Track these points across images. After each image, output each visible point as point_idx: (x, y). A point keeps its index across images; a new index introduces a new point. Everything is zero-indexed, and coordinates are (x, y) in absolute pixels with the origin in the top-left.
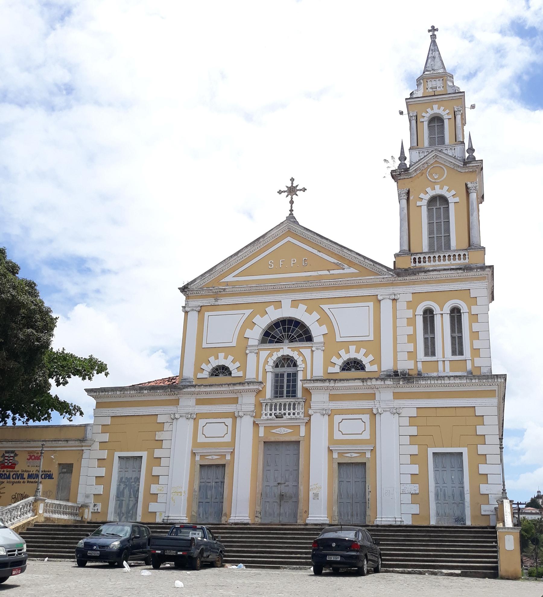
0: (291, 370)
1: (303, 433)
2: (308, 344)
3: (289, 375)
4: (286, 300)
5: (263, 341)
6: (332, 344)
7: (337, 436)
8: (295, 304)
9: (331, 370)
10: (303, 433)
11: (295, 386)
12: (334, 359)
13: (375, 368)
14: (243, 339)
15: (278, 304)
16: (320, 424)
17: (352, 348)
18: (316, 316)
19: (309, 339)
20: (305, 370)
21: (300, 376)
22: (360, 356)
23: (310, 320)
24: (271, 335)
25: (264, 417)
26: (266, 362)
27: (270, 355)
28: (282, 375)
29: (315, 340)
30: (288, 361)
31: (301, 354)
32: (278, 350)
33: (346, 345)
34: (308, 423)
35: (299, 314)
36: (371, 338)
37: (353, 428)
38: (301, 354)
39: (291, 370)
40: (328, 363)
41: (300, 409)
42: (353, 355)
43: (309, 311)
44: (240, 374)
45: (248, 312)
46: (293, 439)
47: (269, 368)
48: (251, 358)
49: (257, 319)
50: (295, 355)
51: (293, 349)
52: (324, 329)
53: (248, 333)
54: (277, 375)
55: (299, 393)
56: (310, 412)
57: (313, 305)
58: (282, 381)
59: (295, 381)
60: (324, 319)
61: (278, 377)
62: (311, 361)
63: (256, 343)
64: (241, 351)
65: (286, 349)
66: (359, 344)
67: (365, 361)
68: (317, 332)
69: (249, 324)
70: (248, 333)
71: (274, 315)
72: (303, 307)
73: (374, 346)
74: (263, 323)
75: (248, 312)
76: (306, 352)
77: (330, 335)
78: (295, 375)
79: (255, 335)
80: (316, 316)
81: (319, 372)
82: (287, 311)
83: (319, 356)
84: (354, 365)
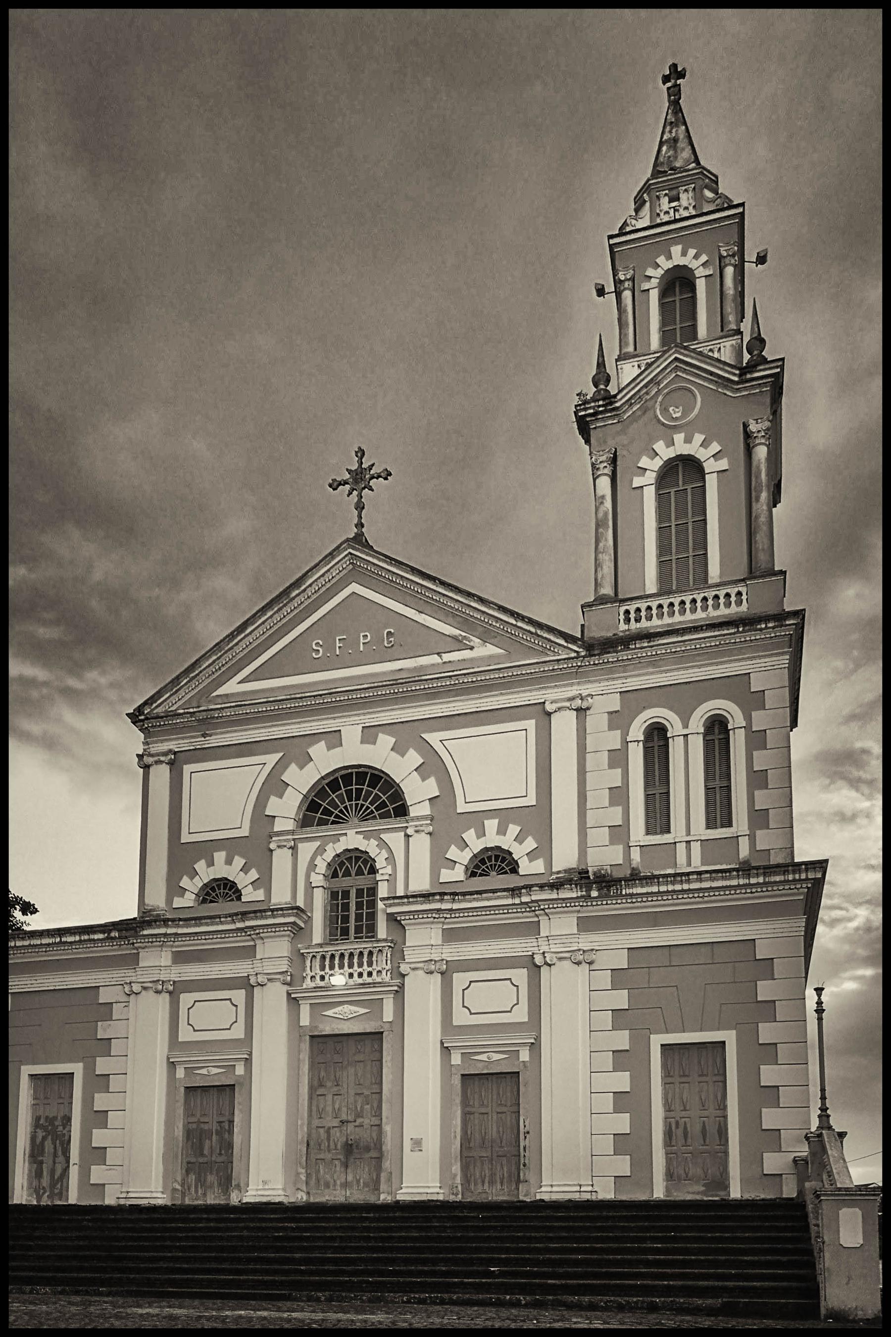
0: (363, 882)
1: (388, 1014)
2: (398, 823)
3: (360, 893)
4: (351, 728)
5: (305, 822)
6: (448, 821)
7: (460, 1017)
8: (369, 734)
9: (446, 875)
10: (388, 1014)
11: (372, 916)
12: (453, 853)
13: (538, 867)
14: (262, 819)
15: (334, 738)
16: (423, 992)
17: (491, 825)
18: (414, 758)
19: (402, 811)
20: (392, 880)
21: (383, 891)
22: (507, 842)
23: (402, 768)
24: (320, 808)
25: (308, 983)
26: (312, 866)
27: (321, 851)
28: (346, 894)
29: (413, 812)
30: (355, 863)
31: (383, 844)
32: (336, 839)
33: (476, 819)
34: (399, 993)
35: (380, 755)
36: (531, 800)
37: (494, 999)
38: (383, 844)
39: (363, 882)
40: (439, 860)
41: (382, 963)
42: (492, 839)
43: (399, 749)
44: (260, 895)
45: (272, 759)
46: (370, 1027)
47: (317, 879)
48: (281, 860)
49: (292, 774)
50: (371, 847)
51: (367, 835)
52: (431, 787)
53: (274, 806)
54: (334, 895)
55: (382, 931)
56: (404, 968)
57: (408, 736)
58: (346, 907)
59: (372, 904)
60: (433, 766)
61: (337, 900)
62: (407, 860)
63: (290, 825)
64: (257, 845)
65: (352, 838)
66: (505, 816)
67: (519, 852)
68: (418, 792)
69: (274, 785)
70: (274, 806)
71: (325, 761)
72: (386, 741)
73: (537, 819)
74: (302, 780)
75: (272, 759)
76: (395, 840)
77: (444, 800)
78: (373, 891)
79: (286, 809)
80: (414, 758)
81: (421, 882)
82: (353, 752)
83: (421, 845)
84: (495, 861)
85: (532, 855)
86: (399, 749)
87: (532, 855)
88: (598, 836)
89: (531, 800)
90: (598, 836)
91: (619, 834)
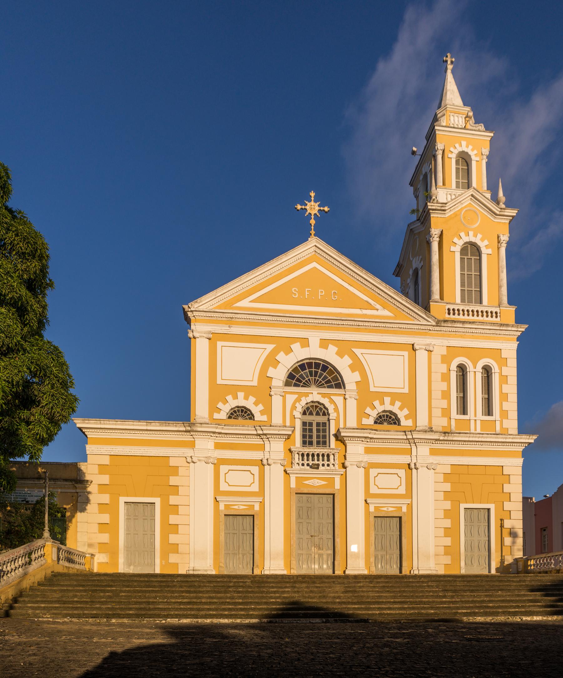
2: (341, 391)
4: (314, 337)
8: (324, 343)
20: (337, 420)
26: (294, 408)
27: (298, 400)
30: (316, 409)
31: (332, 401)
32: (307, 395)
33: (380, 396)
36: (406, 390)
38: (332, 401)
39: (321, 419)
40: (361, 414)
43: (340, 354)
48: (277, 401)
50: (325, 401)
51: (324, 395)
53: (271, 372)
61: (306, 427)
62: (344, 410)
63: (281, 384)
64: (263, 391)
68: (350, 378)
69: (271, 361)
72: (332, 349)
74: (287, 362)
75: (270, 347)
77: (363, 384)
83: (352, 404)
85: (407, 417)
86: (340, 354)
87: (407, 417)
88: (437, 412)
89: (406, 390)
90: (437, 412)
91: (446, 412)
